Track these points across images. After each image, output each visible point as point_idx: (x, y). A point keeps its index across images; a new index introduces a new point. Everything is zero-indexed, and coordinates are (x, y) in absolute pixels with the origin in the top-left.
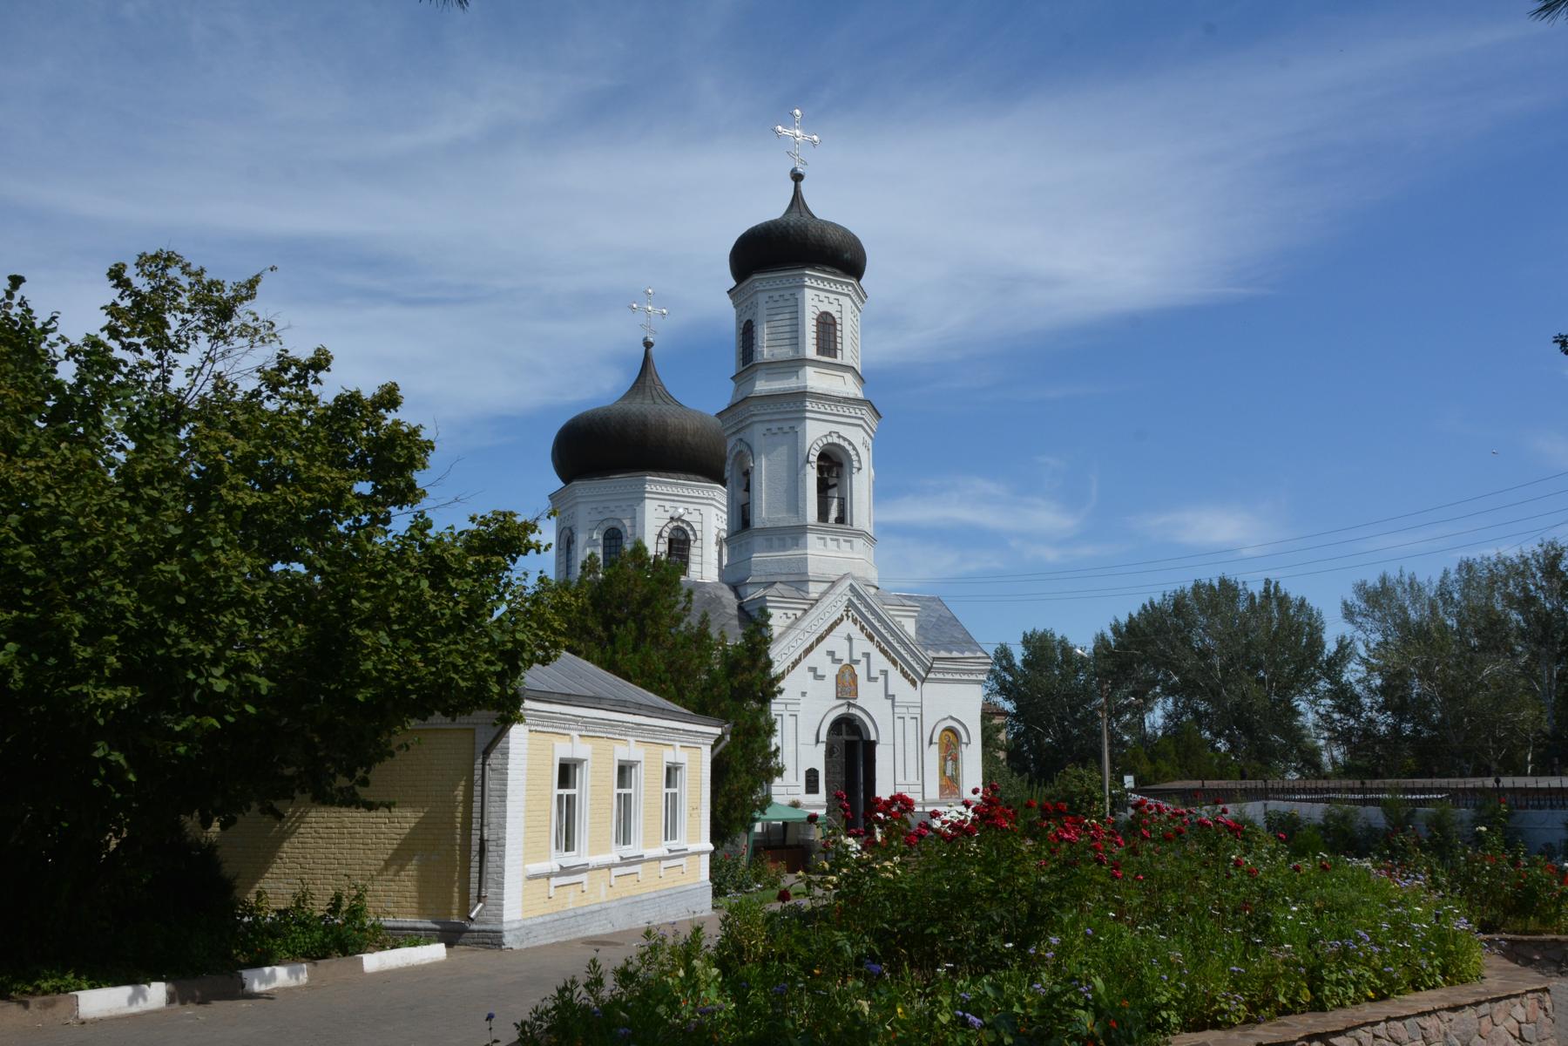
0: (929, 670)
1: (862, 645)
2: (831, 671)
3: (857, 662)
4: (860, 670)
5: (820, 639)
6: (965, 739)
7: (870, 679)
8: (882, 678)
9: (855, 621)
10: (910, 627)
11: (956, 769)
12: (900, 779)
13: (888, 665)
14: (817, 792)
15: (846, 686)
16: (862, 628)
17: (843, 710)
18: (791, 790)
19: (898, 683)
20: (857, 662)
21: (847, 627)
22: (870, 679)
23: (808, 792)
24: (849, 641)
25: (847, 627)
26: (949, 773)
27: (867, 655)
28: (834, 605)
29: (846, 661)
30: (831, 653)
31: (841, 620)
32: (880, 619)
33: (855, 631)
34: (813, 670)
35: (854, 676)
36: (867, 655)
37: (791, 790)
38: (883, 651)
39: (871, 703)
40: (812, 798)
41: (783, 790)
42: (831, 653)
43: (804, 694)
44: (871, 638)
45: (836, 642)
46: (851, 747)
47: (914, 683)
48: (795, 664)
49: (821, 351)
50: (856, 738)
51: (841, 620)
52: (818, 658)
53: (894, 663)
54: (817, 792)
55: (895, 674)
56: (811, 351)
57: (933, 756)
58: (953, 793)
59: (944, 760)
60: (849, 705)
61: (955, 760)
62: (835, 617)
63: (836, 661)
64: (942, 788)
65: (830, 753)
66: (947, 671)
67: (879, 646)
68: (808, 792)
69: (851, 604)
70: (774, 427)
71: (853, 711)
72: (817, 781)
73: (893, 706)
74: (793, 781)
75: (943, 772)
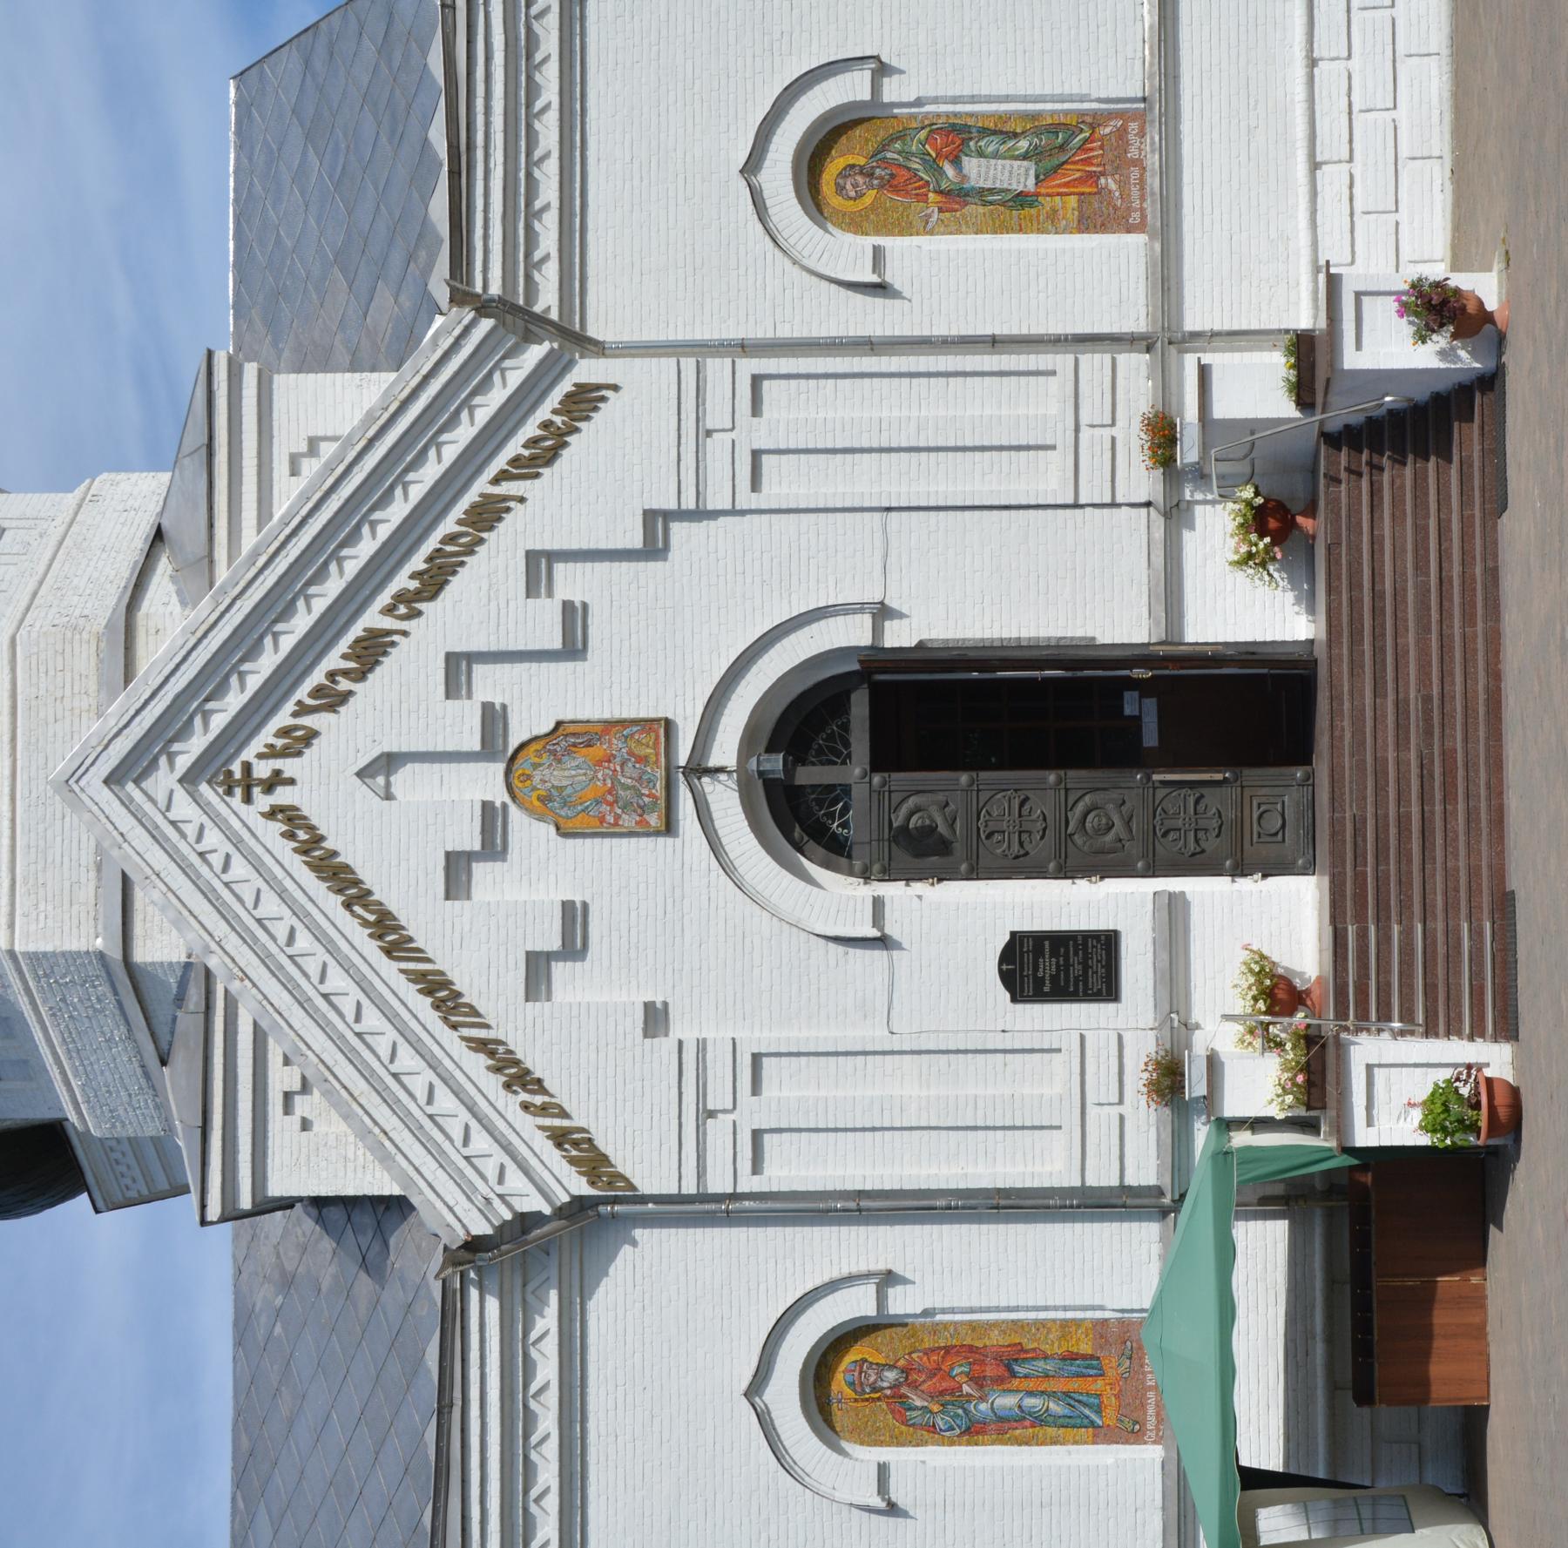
0: (516, 319)
1: (401, 700)
2: (545, 868)
3: (494, 719)
4: (538, 701)
6: (852, 88)
7: (573, 647)
8: (570, 582)
9: (298, 742)
10: (329, 407)
11: (1000, 130)
12: (1050, 479)
13: (501, 554)
14: (1108, 942)
15: (609, 778)
16: (331, 699)
17: (725, 799)
18: (1101, 1084)
19: (584, 497)
20: (494, 719)
21: (322, 783)
22: (573, 647)
23: (1108, 990)
24: (392, 772)
25: (322, 783)
26: (1017, 175)
27: (458, 670)
29: (488, 782)
30: (456, 873)
31: (290, 817)
32: (277, 606)
33: (345, 738)
34: (537, 971)
35: (566, 737)
36: (458, 670)
38: (434, 581)
39: (691, 647)
40: (1137, 966)
41: (1101, 1120)
42: (456, 873)
43: (655, 1019)
44: (371, 651)
45: (395, 846)
46: (906, 750)
47: (584, 401)
48: (520, 1078)
50: (860, 705)
51: (290, 817)
52: (476, 944)
53: (487, 515)
54: (1108, 942)
55: (548, 510)
58: (1122, 163)
59: (957, 197)
60: (698, 769)
61: (958, 136)
62: (285, 850)
63: (494, 842)
64: (1098, 217)
65: (923, 853)
66: (521, 193)
67: (408, 604)
68: (1108, 990)
69: (216, 770)
71: (725, 751)
72: (1060, 942)
73: (700, 514)
74: (1062, 1068)
75: (1016, 211)
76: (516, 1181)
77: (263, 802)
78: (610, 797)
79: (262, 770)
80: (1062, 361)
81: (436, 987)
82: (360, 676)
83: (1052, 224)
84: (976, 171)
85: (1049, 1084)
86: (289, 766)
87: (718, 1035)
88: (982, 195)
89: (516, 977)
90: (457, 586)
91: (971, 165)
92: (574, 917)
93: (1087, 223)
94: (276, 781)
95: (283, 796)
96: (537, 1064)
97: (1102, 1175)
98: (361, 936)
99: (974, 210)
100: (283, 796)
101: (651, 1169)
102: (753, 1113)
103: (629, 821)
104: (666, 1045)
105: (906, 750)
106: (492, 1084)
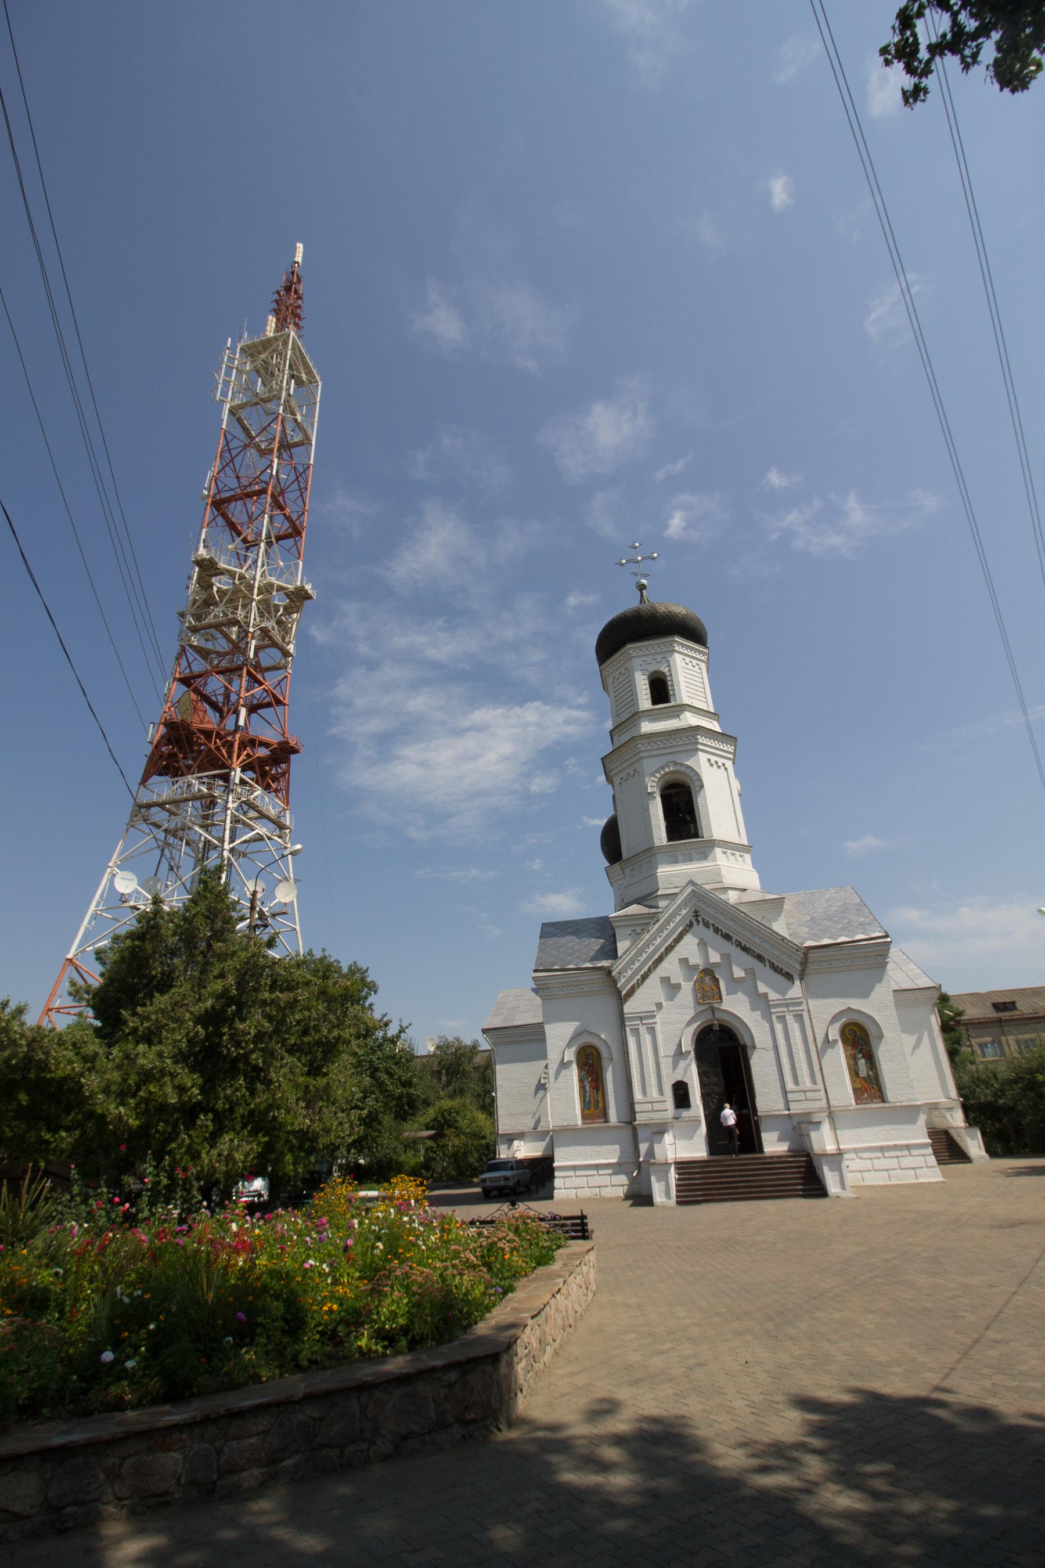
5: (669, 949)
9: (706, 925)
12: (790, 1086)
17: (707, 1017)
18: (656, 1106)
28: (672, 914)
34: (666, 980)
37: (656, 1106)
38: (745, 949)
44: (727, 937)
46: (723, 1056)
47: (789, 977)
48: (644, 977)
49: (655, 701)
52: (670, 967)
53: (760, 958)
56: (645, 701)
57: (838, 1057)
67: (739, 944)
70: (624, 775)
71: (718, 1015)
75: (854, 1073)
76: (623, 981)
77: (693, 920)
78: (704, 991)
79: (700, 919)
80: (820, 1086)
81: (661, 959)
82: (722, 935)
83: (853, 1082)
84: (862, 1062)
85: (654, 1093)
86: (701, 924)
87: (657, 1019)
88: (856, 1064)
89: (664, 975)
90: (744, 954)
91: (863, 1061)
92: (678, 987)
93: (855, 1090)
94: (698, 922)
95: (695, 923)
96: (648, 981)
97: (637, 1108)
98: (669, 942)
99: (852, 1062)
100: (695, 923)
101: (629, 1008)
102: (643, 1030)
103: (699, 995)
104: (655, 1008)
105: (723, 1056)
106: (642, 972)
